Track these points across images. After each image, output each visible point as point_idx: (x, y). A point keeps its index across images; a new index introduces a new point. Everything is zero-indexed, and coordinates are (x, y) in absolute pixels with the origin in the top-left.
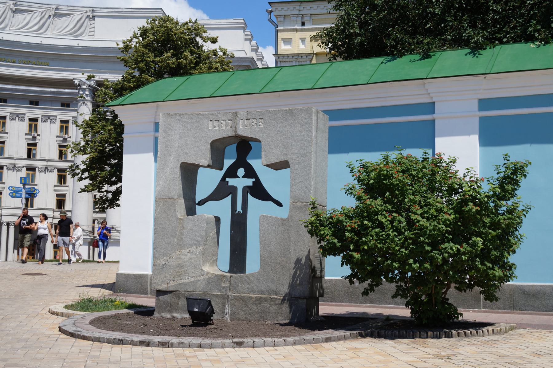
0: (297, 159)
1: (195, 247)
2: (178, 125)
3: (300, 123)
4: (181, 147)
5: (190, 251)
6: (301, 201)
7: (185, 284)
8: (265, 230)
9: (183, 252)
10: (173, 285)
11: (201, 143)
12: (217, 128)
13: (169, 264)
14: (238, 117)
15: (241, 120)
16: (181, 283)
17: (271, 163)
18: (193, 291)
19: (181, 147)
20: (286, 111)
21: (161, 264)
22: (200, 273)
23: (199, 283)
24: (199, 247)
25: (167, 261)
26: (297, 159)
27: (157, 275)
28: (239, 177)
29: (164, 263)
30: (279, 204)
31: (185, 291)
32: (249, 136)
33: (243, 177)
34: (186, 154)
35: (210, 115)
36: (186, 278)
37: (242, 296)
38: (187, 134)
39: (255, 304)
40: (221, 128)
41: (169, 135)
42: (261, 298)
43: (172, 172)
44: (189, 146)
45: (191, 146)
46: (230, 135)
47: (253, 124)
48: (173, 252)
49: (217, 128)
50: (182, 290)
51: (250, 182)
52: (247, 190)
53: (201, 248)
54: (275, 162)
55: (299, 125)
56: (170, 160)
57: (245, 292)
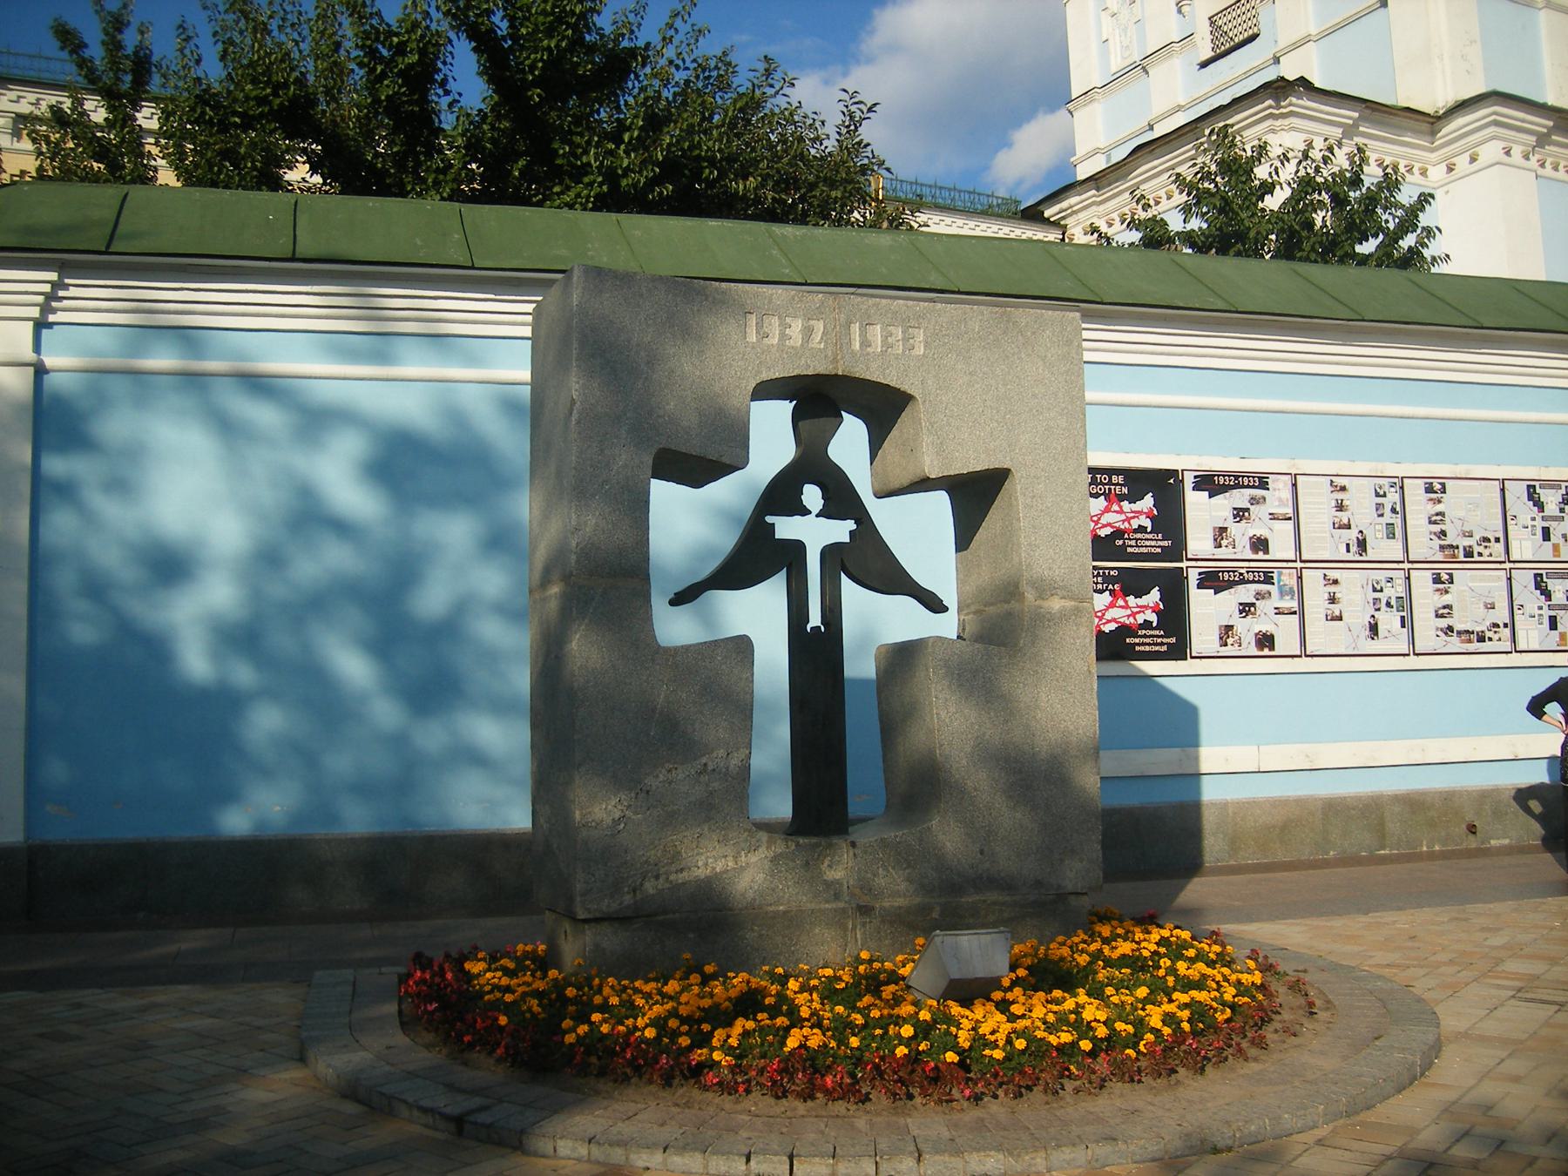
3: (1044, 359)
5: (705, 765)
9: (680, 774)
21: (609, 821)
24: (738, 749)
28: (805, 512)
29: (617, 815)
30: (933, 604)
36: (700, 864)
51: (841, 531)
52: (832, 554)
55: (1040, 363)
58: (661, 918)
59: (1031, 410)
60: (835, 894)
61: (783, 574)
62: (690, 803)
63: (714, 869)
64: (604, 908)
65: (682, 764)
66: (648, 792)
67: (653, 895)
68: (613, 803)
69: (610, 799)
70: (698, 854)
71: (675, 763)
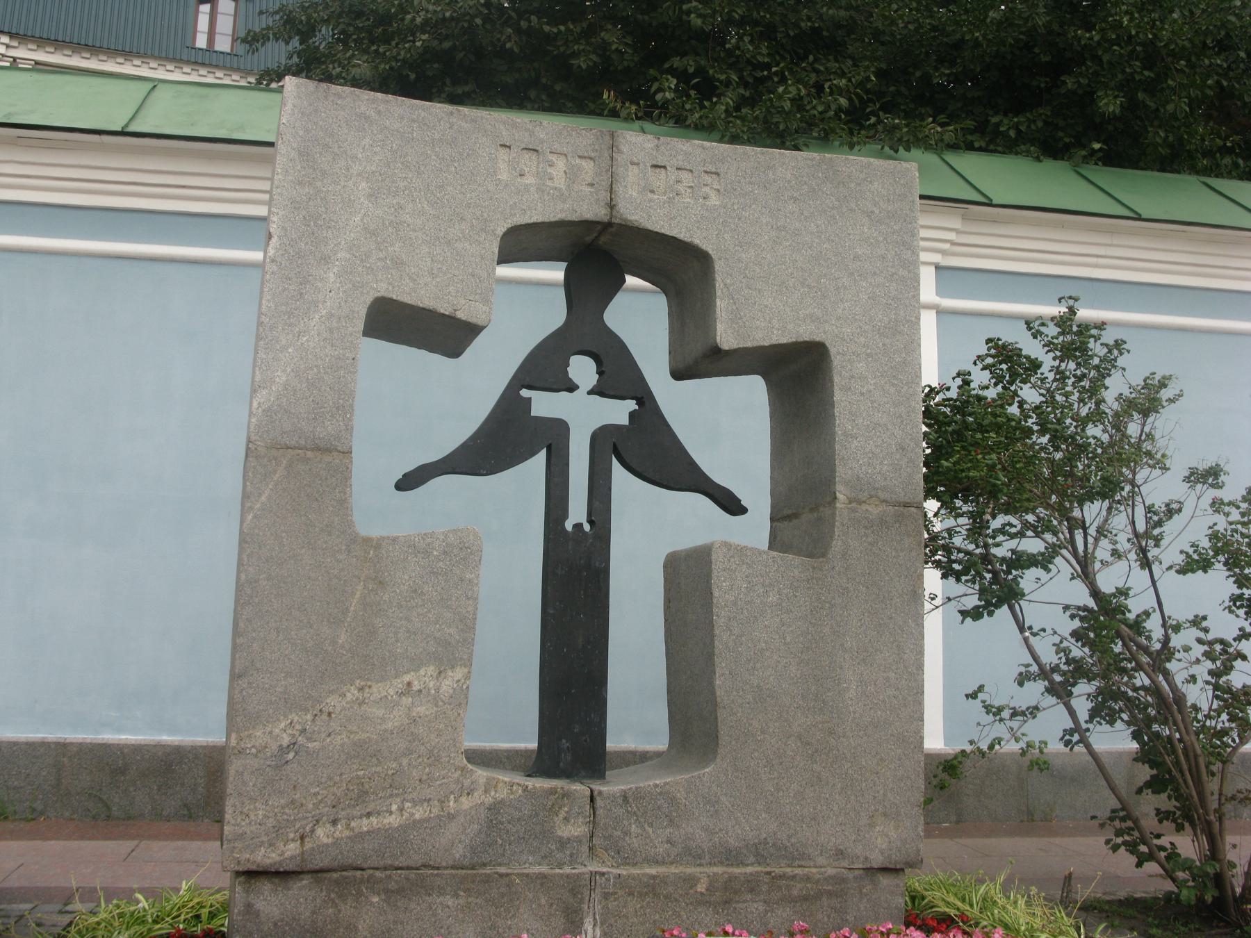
0: (862, 340)
1: (431, 670)
2: (367, 141)
3: (870, 214)
4: (373, 234)
5: (409, 684)
6: (882, 495)
7: (388, 834)
8: (735, 603)
9: (378, 690)
10: (330, 840)
11: (463, 232)
12: (529, 180)
13: (309, 745)
14: (620, 152)
15: (633, 163)
16: (368, 832)
17: (755, 344)
18: (425, 866)
19: (373, 234)
20: (809, 162)
21: (274, 747)
22: (457, 781)
23: (453, 827)
24: (453, 667)
25: (303, 731)
26: (862, 340)
27: (251, 798)
28: (572, 388)
29: (286, 740)
30: (731, 504)
31: (385, 869)
32: (663, 231)
33: (597, 391)
34: (398, 263)
35: (502, 127)
36: (394, 807)
37: (654, 877)
38: (402, 184)
39: (708, 903)
40: (549, 183)
41: (324, 173)
42: (732, 878)
43: (331, 330)
44: (413, 235)
45: (419, 234)
46: (589, 216)
47: (680, 188)
48: (331, 692)
49: (529, 180)
50: (369, 863)
51: (619, 412)
53: (459, 673)
54: (774, 341)
56: (321, 279)
57: (660, 858)
58: (335, 875)
59: (852, 274)
60: (571, 856)
61: (541, 457)
62: (386, 731)
63: (413, 814)
64: (259, 859)
65: (377, 682)
66: (329, 714)
67: (327, 845)
68: (282, 725)
69: (279, 720)
70: (391, 796)
71: (368, 680)
